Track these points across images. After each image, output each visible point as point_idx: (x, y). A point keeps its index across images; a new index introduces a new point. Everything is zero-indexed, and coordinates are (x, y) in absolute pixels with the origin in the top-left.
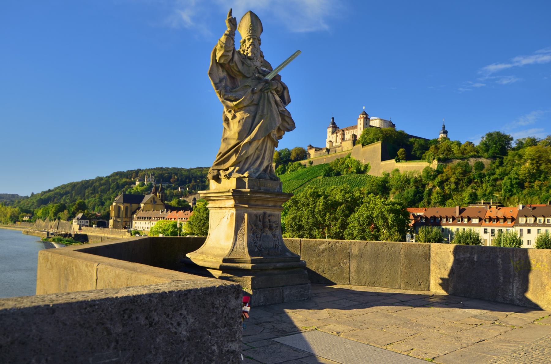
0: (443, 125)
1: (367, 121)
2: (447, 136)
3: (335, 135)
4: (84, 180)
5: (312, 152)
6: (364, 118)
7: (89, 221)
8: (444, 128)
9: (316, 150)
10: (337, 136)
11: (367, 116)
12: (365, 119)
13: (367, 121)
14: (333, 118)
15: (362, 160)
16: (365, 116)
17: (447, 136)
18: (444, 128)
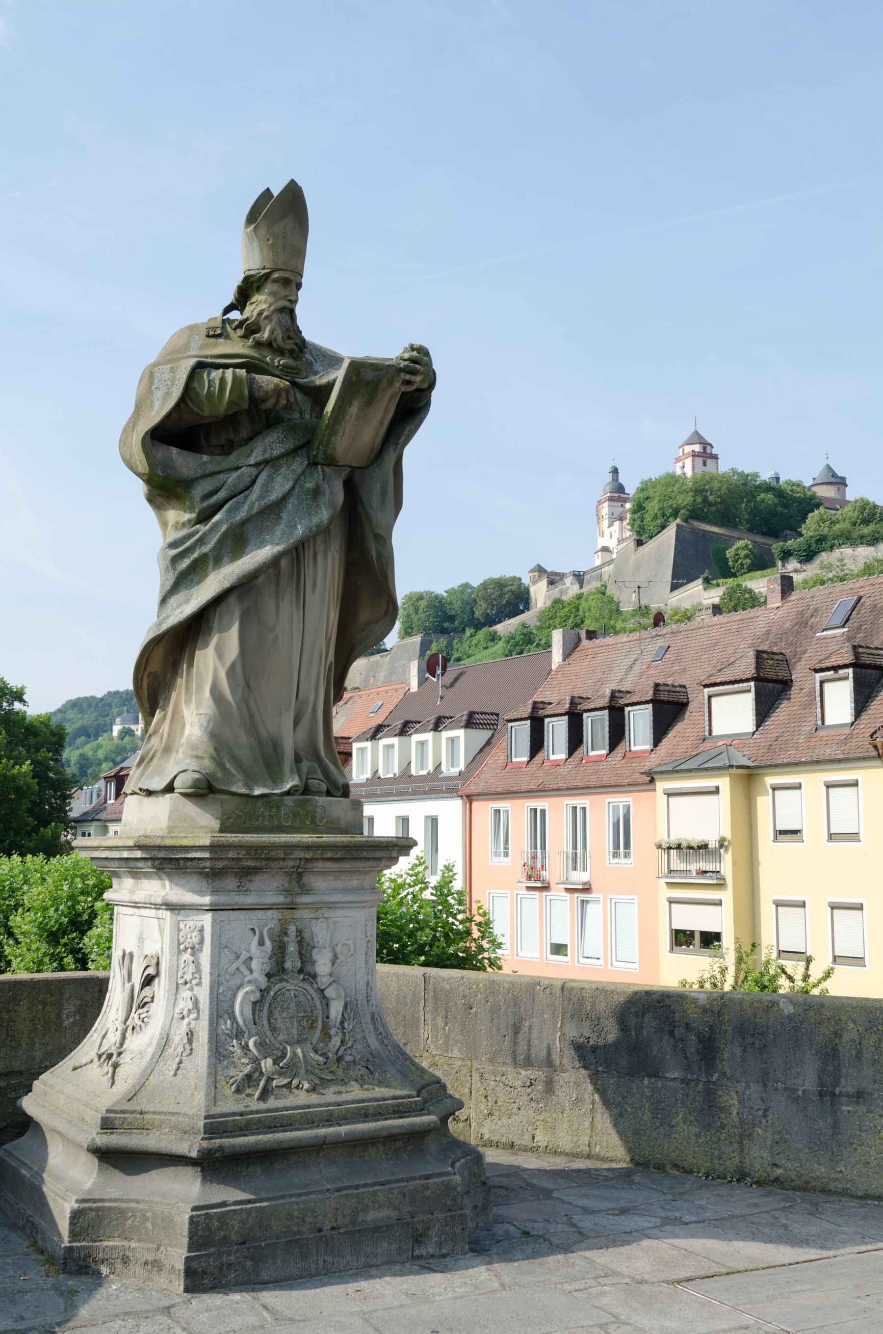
1: (705, 464)
9: (551, 583)
11: (705, 448)
12: (699, 461)
13: (705, 464)
15: (631, 597)
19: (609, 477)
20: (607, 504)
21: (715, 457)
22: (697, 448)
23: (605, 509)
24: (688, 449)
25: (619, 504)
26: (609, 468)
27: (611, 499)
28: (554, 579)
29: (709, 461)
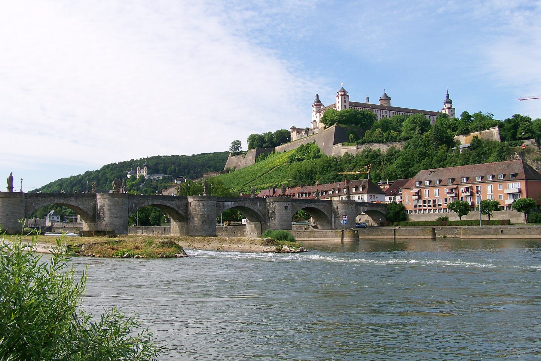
0: (446, 94)
1: (345, 98)
2: (451, 106)
3: (318, 114)
4: (57, 180)
5: (294, 135)
6: (342, 95)
7: (59, 217)
8: (448, 96)
9: (298, 132)
10: (320, 115)
11: (345, 93)
13: (345, 98)
14: (317, 96)
16: (343, 93)
17: (451, 106)
18: (448, 96)
19: (316, 98)
20: (315, 107)
21: (348, 96)
22: (343, 93)
23: (314, 108)
24: (340, 93)
25: (319, 107)
26: (316, 95)
27: (316, 105)
28: (299, 131)
29: (346, 97)
